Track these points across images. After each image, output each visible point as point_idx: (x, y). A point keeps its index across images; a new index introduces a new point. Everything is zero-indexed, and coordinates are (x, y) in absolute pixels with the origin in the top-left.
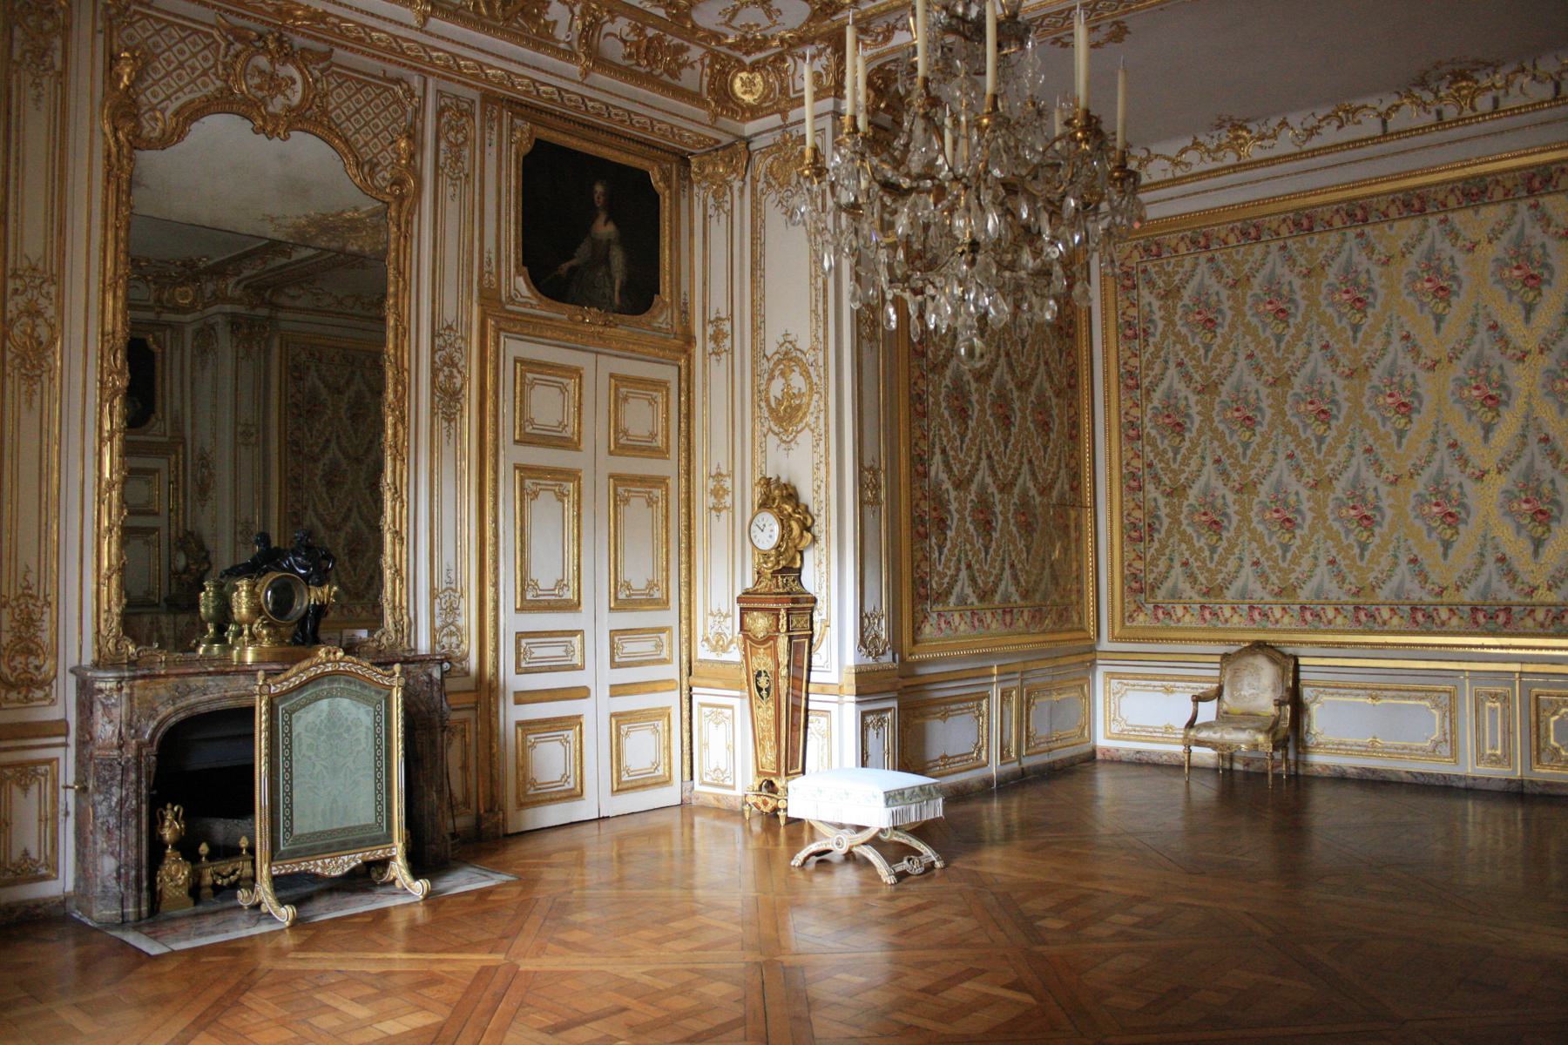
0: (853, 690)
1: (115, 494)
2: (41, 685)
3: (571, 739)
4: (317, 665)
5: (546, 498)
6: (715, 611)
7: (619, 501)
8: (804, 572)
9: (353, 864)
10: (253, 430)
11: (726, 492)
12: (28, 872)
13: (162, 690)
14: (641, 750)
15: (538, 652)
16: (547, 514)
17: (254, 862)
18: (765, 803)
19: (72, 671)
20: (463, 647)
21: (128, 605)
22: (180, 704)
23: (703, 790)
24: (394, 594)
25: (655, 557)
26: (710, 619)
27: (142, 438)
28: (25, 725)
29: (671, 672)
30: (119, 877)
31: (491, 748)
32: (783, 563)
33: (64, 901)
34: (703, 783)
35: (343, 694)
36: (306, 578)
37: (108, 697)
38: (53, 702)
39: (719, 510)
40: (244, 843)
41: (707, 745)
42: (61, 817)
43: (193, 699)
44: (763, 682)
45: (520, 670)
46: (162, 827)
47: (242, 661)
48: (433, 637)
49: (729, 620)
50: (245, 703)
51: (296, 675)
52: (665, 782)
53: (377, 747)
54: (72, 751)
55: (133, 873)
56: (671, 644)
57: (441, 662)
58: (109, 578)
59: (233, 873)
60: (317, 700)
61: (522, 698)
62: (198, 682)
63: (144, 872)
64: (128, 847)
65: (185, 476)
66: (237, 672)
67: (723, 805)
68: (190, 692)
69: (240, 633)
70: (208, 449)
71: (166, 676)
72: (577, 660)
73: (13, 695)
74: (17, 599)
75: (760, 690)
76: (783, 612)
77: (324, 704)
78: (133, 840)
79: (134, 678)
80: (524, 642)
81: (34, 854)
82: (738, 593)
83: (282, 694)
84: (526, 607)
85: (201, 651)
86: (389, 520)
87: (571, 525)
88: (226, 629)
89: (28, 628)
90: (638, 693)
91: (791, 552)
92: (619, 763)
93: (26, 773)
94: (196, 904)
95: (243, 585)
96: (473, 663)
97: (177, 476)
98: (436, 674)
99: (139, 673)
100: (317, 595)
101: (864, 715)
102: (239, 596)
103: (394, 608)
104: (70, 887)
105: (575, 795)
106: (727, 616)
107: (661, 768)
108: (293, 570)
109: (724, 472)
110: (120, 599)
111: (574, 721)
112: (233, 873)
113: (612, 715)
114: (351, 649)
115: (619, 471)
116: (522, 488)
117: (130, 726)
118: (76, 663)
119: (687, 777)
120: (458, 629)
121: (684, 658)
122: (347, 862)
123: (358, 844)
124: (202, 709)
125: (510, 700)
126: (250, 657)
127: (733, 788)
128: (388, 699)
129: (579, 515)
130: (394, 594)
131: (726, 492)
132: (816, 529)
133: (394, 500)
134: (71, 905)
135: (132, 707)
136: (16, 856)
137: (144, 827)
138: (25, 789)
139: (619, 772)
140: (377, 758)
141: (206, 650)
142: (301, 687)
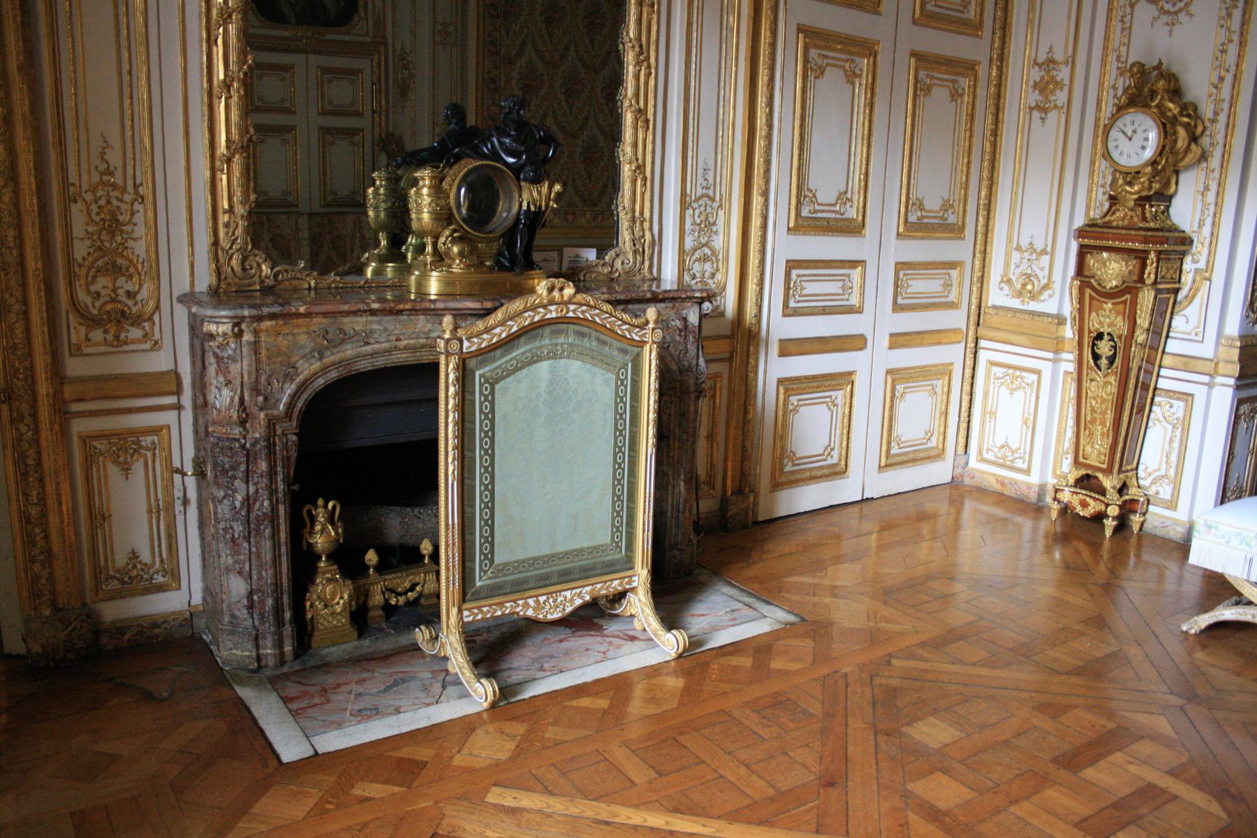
0: (1236, 369)
1: (232, 29)
2: (137, 321)
3: (840, 401)
4: (534, 308)
5: (833, 77)
6: (1024, 243)
7: (921, 90)
8: (1174, 200)
9: (578, 602)
10: (451, 29)
11: (1059, 85)
12: (137, 581)
13: (302, 336)
14: (917, 416)
15: (811, 288)
16: (835, 99)
17: (438, 573)
18: (1084, 505)
19: (180, 300)
20: (719, 276)
21: (258, 204)
22: (330, 358)
23: (981, 468)
24: (634, 201)
25: (954, 169)
26: (1016, 256)
27: (347, 38)
28: (117, 378)
29: (957, 319)
30: (251, 607)
31: (746, 412)
32: (1156, 186)
33: (191, 617)
34: (982, 460)
35: (572, 353)
36: (516, 170)
37: (222, 347)
38: (156, 345)
39: (1045, 110)
40: (426, 547)
41: (993, 414)
42: (178, 507)
43: (349, 350)
44: (1104, 348)
45: (788, 312)
46: (312, 532)
47: (422, 294)
48: (681, 262)
49: (1045, 260)
50: (426, 358)
51: (502, 323)
52: (936, 455)
53: (619, 433)
54: (188, 415)
55: (270, 602)
56: (960, 284)
57: (700, 302)
58: (229, 161)
59: (412, 589)
60: (531, 362)
61: (789, 348)
62: (358, 324)
63: (286, 600)
64: (261, 566)
65: (387, 79)
66: (414, 311)
67: (1009, 491)
68: (345, 338)
69: (420, 249)
70: (408, 50)
71: (308, 315)
72: (854, 300)
73: (97, 335)
74: (93, 190)
75: (1096, 357)
76: (1152, 255)
77: (544, 367)
78: (268, 556)
79: (260, 319)
80: (794, 273)
81: (145, 556)
82: (1079, 222)
83: (480, 353)
84: (803, 226)
85: (369, 272)
86: (630, 92)
87: (860, 118)
88: (404, 242)
89: (112, 234)
90: (921, 345)
91: (1168, 173)
92: (890, 431)
93: (126, 447)
94: (361, 634)
95: (425, 176)
96: (729, 302)
97: (379, 78)
98: (693, 318)
99: (266, 310)
100: (532, 196)
101: (1240, 402)
102: (418, 193)
103: (633, 219)
104: (197, 599)
105: (837, 472)
106: (1044, 252)
107: (934, 439)
108: (495, 156)
109: (1059, 56)
110: (246, 193)
111: (843, 379)
112: (412, 589)
113: (889, 372)
114: (574, 274)
115: (922, 48)
116: (806, 61)
117: (256, 390)
118: (187, 289)
119: (961, 450)
120: (714, 252)
121: (974, 301)
122: (572, 598)
123: (586, 573)
124: (365, 366)
125: (774, 349)
126: (434, 286)
127: (1027, 472)
128: (637, 362)
129: (872, 105)
130: (634, 201)
131: (1059, 85)
132: (1205, 141)
133: (638, 63)
134: (200, 623)
135: (258, 361)
136: (121, 559)
137: (283, 536)
138: (126, 469)
139: (889, 443)
140: (618, 449)
141: (377, 272)
142: (510, 342)
